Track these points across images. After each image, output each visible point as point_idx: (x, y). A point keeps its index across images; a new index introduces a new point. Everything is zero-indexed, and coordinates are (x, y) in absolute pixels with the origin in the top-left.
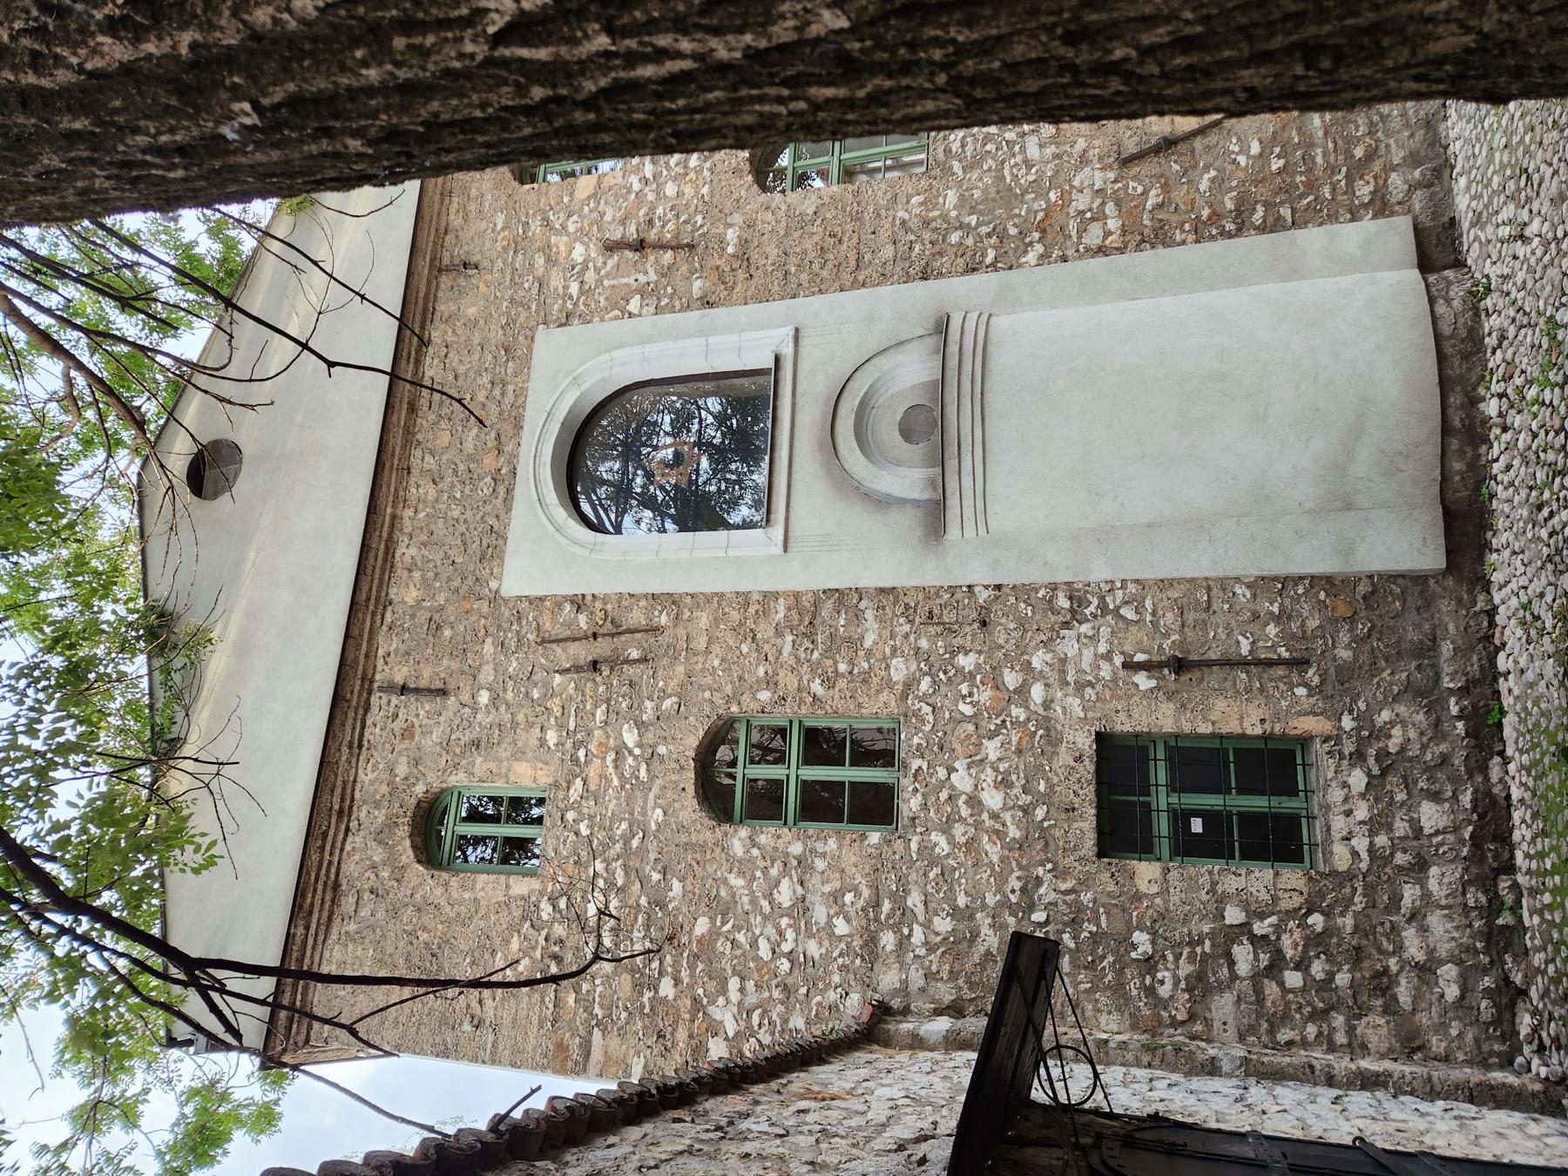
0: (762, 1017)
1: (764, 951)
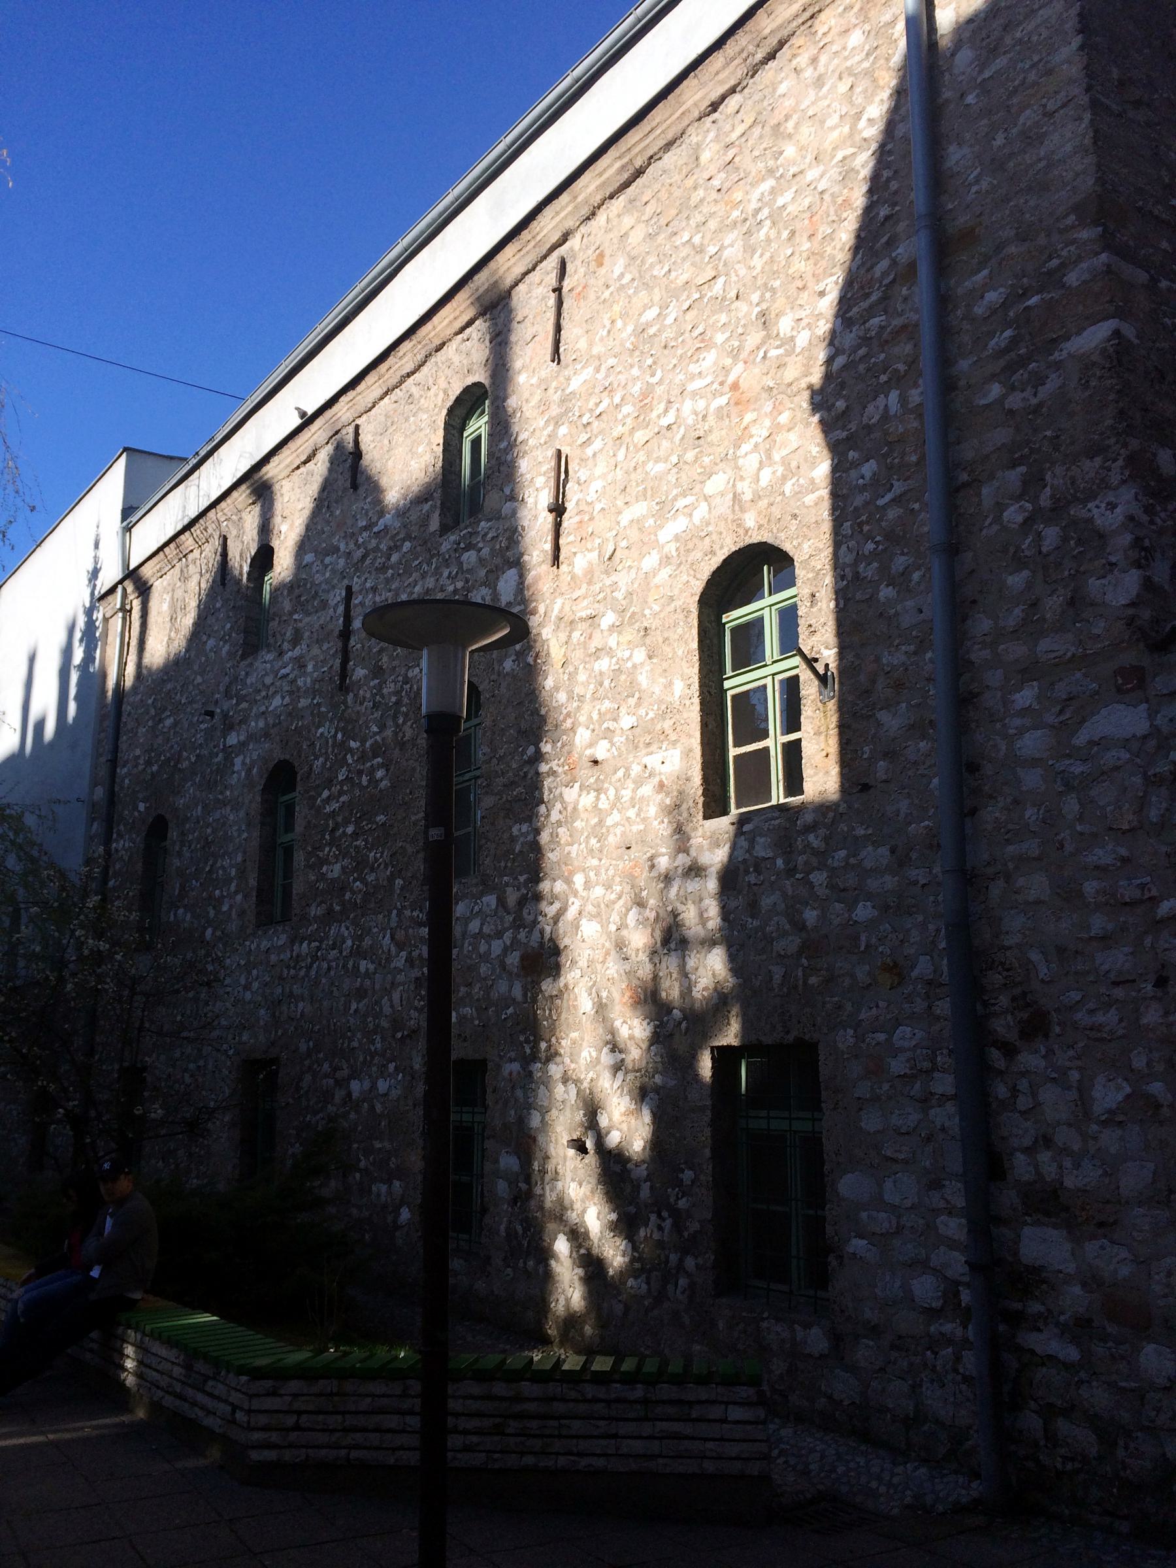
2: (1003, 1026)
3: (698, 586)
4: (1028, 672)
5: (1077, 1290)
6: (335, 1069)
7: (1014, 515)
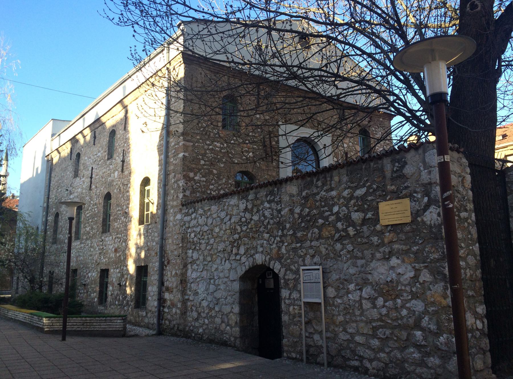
1: (211, 187)
2: (166, 263)
4: (172, 207)
6: (86, 271)
7: (173, 181)
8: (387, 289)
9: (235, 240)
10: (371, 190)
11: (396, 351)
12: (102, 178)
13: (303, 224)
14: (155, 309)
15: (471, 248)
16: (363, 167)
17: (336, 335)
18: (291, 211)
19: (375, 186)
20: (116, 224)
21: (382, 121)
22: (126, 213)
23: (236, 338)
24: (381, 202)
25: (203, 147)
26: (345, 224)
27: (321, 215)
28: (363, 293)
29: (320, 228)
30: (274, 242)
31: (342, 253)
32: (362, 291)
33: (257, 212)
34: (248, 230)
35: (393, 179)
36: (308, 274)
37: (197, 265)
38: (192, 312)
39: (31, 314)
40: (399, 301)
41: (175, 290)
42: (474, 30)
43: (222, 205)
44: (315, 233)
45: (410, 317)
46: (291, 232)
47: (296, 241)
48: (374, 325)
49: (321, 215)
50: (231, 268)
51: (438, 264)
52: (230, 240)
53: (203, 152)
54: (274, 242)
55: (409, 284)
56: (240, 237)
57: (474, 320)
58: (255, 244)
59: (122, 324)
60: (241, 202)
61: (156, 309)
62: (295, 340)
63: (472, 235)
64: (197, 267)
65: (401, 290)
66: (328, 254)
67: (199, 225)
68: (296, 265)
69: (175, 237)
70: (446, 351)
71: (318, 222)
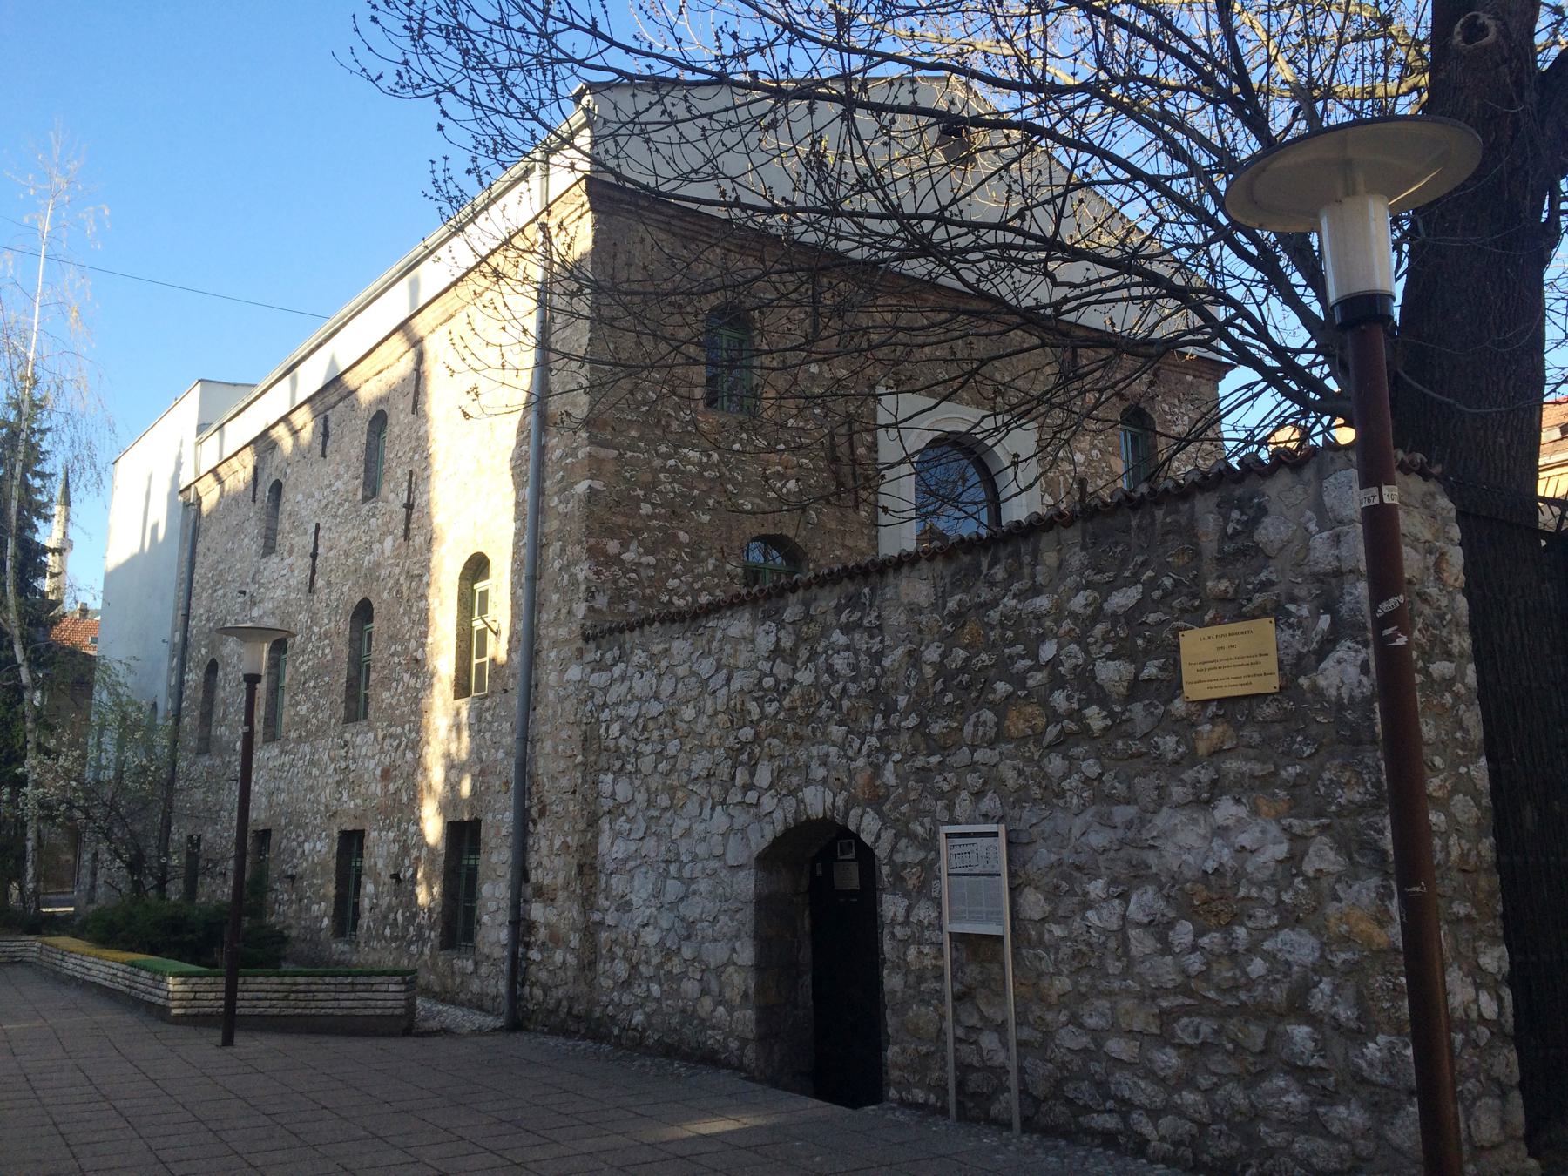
0: (634, 580)
1: (672, 583)
2: (534, 812)
3: (459, 570)
4: (555, 643)
5: (542, 930)
6: (298, 836)
7: (557, 566)
8: (1205, 894)
9: (744, 745)
10: (1157, 594)
11: (1230, 1085)
12: (347, 556)
13: (949, 697)
14: (501, 953)
15: (1463, 770)
16: (1134, 523)
17: (1048, 1035)
18: (914, 657)
19: (1168, 582)
20: (386, 694)
21: (1191, 384)
22: (417, 661)
23: (744, 1042)
24: (1186, 629)
25: (648, 462)
26: (1077, 695)
27: (1003, 667)
28: (1132, 907)
29: (1001, 708)
30: (860, 749)
31: (1066, 785)
32: (1127, 902)
33: (809, 660)
34: (781, 716)
35: (1222, 559)
36: (963, 849)
37: (630, 820)
38: (613, 960)
39: (132, 964)
40: (1241, 932)
41: (561, 896)
42: (1476, 102)
43: (705, 638)
44: (984, 724)
45: (1275, 981)
46: (912, 721)
47: (928, 747)
48: (1165, 1004)
49: (1003, 667)
50: (730, 829)
51: (1361, 821)
52: (727, 744)
53: (648, 477)
54: (860, 749)
55: (1272, 881)
56: (757, 734)
57: (1471, 991)
58: (802, 755)
59: (402, 996)
60: (760, 630)
61: (505, 953)
62: (924, 1049)
63: (1466, 731)
64: (627, 826)
65: (1247, 898)
66: (1026, 787)
67: (635, 698)
68: (927, 820)
69: (564, 735)
70: (1384, 1086)
71: (994, 691)
